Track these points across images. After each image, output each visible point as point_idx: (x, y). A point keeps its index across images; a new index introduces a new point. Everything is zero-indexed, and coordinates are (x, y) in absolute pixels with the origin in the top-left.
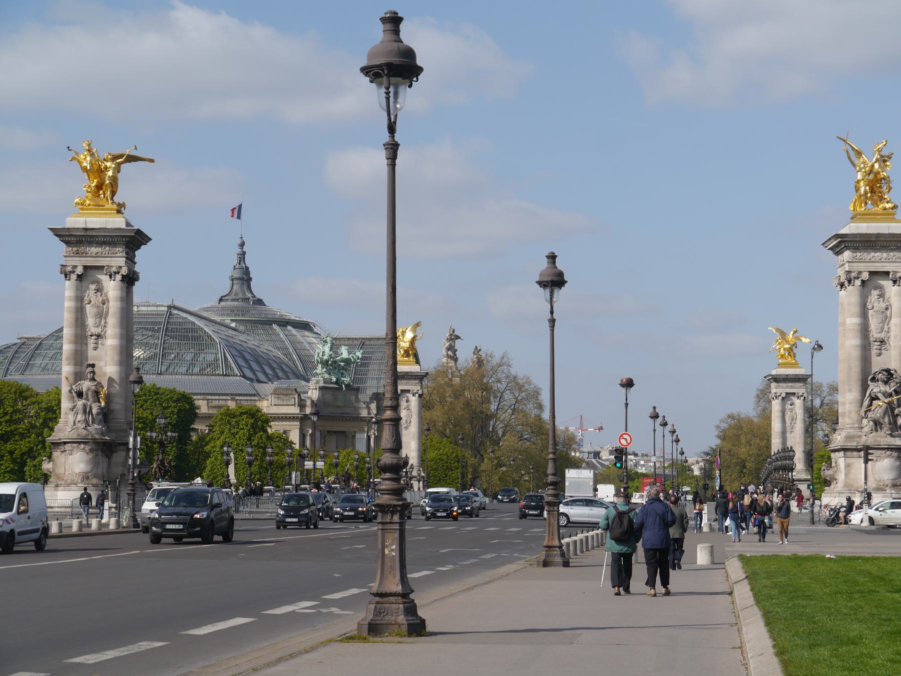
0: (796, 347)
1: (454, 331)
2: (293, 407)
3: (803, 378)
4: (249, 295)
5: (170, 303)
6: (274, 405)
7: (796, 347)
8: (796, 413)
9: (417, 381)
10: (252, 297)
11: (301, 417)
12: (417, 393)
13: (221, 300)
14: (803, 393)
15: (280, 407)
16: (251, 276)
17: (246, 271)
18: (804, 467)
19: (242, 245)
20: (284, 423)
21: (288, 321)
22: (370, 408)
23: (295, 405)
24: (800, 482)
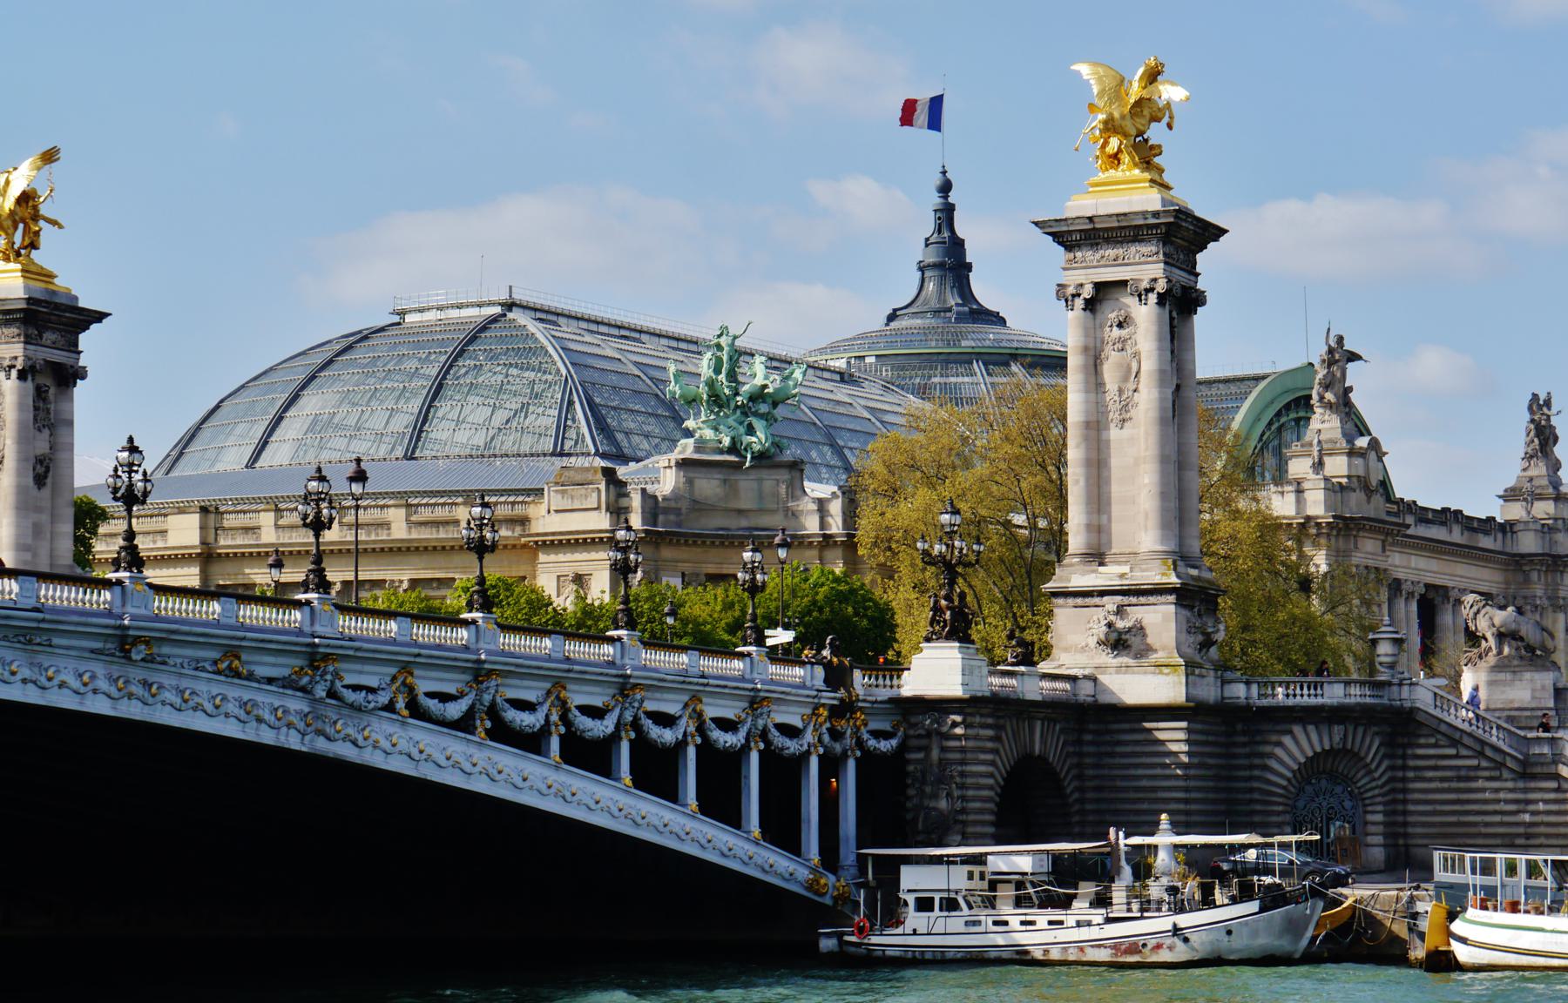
0: (1170, 126)
1: (1340, 339)
2: (595, 513)
3: (1150, 227)
4: (953, 300)
5: (504, 296)
6: (557, 511)
7: (1170, 126)
8: (1136, 355)
9: (14, 330)
10: (957, 305)
11: (608, 538)
12: (14, 366)
13: (892, 317)
14: (1155, 280)
15: (567, 514)
16: (968, 260)
17: (955, 246)
18: (1162, 544)
19: (945, 188)
20: (578, 556)
21: (1013, 351)
22: (828, 511)
23: (598, 508)
24: (1143, 600)
